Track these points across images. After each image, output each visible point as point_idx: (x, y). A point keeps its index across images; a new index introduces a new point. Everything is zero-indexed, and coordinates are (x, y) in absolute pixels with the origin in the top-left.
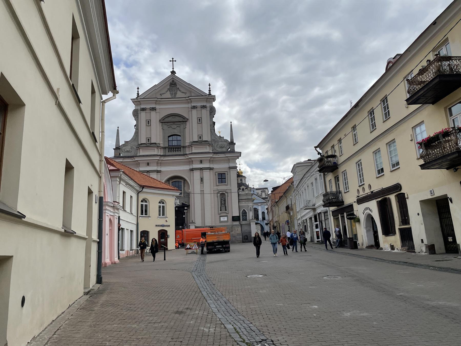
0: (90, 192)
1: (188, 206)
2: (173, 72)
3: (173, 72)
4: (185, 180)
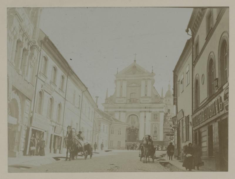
0: (77, 124)
1: (138, 130)
2: (135, 61)
3: (135, 61)
4: (137, 116)
